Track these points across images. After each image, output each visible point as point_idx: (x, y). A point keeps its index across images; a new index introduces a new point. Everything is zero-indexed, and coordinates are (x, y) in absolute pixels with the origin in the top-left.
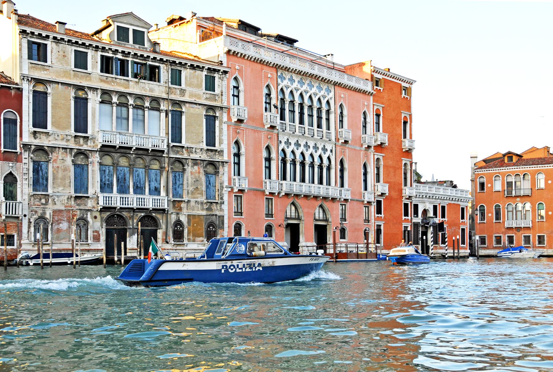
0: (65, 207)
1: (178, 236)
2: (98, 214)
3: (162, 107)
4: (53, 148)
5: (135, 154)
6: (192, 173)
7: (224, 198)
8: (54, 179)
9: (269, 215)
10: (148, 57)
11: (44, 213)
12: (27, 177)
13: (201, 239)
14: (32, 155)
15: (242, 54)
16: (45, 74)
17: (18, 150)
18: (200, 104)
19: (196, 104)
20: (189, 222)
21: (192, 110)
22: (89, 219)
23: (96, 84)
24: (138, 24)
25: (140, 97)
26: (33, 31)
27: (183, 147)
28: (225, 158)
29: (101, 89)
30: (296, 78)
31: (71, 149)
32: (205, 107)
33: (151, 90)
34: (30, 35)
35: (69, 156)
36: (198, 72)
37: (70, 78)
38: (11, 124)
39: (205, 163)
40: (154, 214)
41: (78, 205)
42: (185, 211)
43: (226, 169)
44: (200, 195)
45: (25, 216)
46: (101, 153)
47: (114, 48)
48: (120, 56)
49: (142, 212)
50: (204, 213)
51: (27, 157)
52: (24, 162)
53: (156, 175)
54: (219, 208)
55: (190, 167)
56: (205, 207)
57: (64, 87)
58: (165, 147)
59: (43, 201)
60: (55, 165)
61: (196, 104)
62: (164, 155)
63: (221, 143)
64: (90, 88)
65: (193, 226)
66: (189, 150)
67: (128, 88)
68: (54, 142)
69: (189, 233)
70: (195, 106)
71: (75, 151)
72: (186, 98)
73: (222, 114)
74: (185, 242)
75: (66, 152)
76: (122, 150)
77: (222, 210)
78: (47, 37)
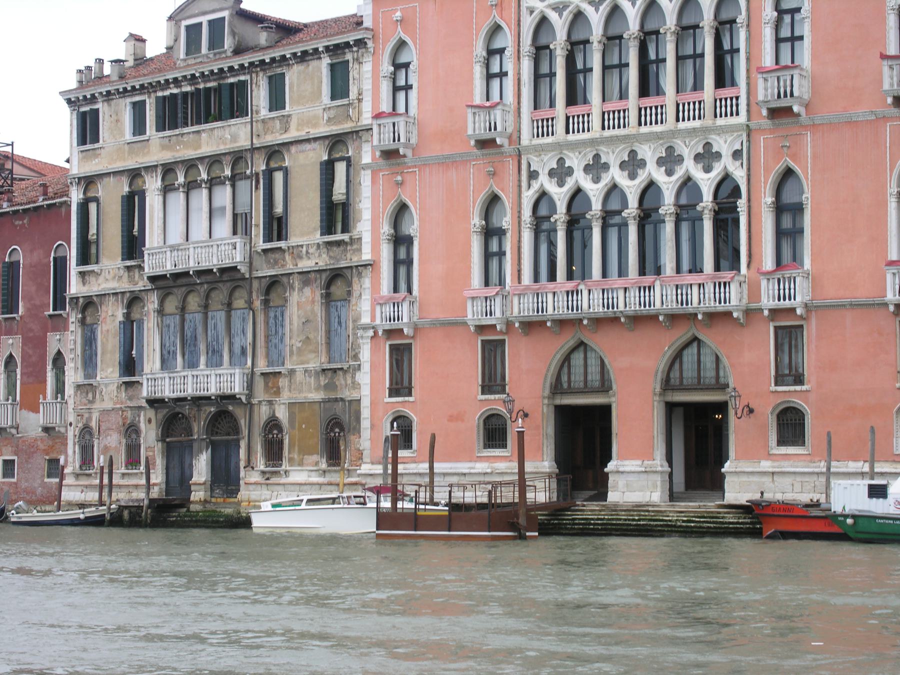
0: (115, 403)
1: (274, 452)
2: (151, 413)
4: (101, 296)
5: (207, 283)
6: (303, 303)
7: (361, 356)
8: (103, 353)
9: (492, 382)
10: (221, 70)
11: (90, 419)
13: (315, 458)
16: (96, 164)
18: (316, 139)
19: (308, 141)
21: (301, 157)
22: (142, 426)
23: (155, 158)
25: (214, 160)
28: (366, 255)
29: (162, 165)
32: (327, 142)
36: (314, 64)
37: (124, 160)
38: (61, 265)
39: (324, 276)
40: (231, 408)
41: (130, 398)
42: (286, 396)
43: (367, 282)
44: (313, 355)
45: (71, 424)
46: (160, 292)
48: (187, 89)
49: (212, 405)
52: (71, 329)
53: (244, 319)
54: (349, 381)
55: (296, 293)
56: (323, 381)
59: (90, 396)
60: (105, 328)
61: (308, 141)
64: (147, 168)
66: (296, 252)
67: (199, 147)
70: (307, 146)
71: (128, 295)
72: (293, 134)
73: (359, 148)
74: (285, 466)
76: (184, 281)
77: (356, 386)
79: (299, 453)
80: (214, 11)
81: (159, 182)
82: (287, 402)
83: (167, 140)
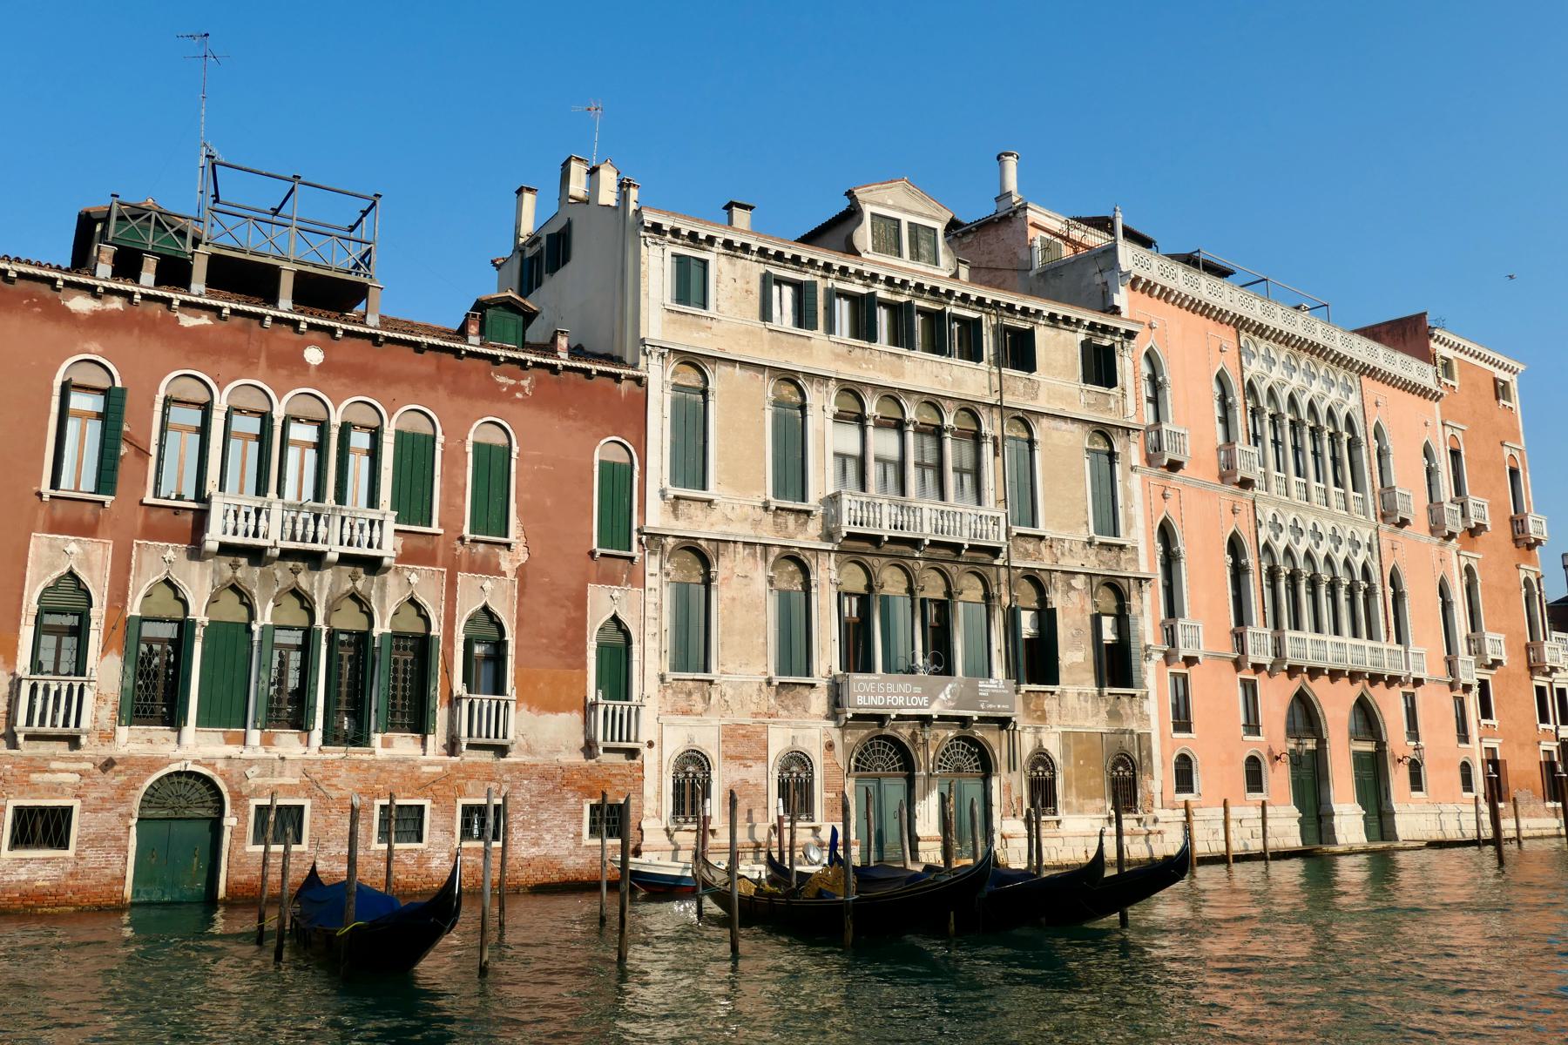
3: (985, 429)
10: (949, 293)
12: (656, 630)
13: (1099, 803)
14: (668, 566)
15: (1163, 289)
17: (635, 550)
20: (1065, 756)
21: (1055, 434)
24: (920, 209)
26: (677, 226)
27: (1041, 538)
28: (1144, 569)
30: (1282, 353)
31: (766, 546)
33: (957, 382)
34: (669, 236)
35: (761, 564)
39: (1095, 581)
40: (978, 733)
43: (1147, 596)
45: (651, 744)
47: (868, 269)
50: (1103, 728)
51: (656, 570)
52: (648, 585)
54: (1136, 711)
57: (750, 373)
58: (1003, 538)
62: (997, 562)
63: (1129, 527)
64: (810, 376)
65: (1077, 764)
67: (902, 375)
68: (724, 528)
69: (1067, 786)
71: (777, 550)
72: (1040, 405)
73: (1126, 447)
75: (754, 556)
76: (894, 548)
77: (1144, 718)
78: (711, 240)
79: (1078, 796)
80: (921, 215)
81: (832, 408)
82: (1060, 730)
83: (846, 349)
